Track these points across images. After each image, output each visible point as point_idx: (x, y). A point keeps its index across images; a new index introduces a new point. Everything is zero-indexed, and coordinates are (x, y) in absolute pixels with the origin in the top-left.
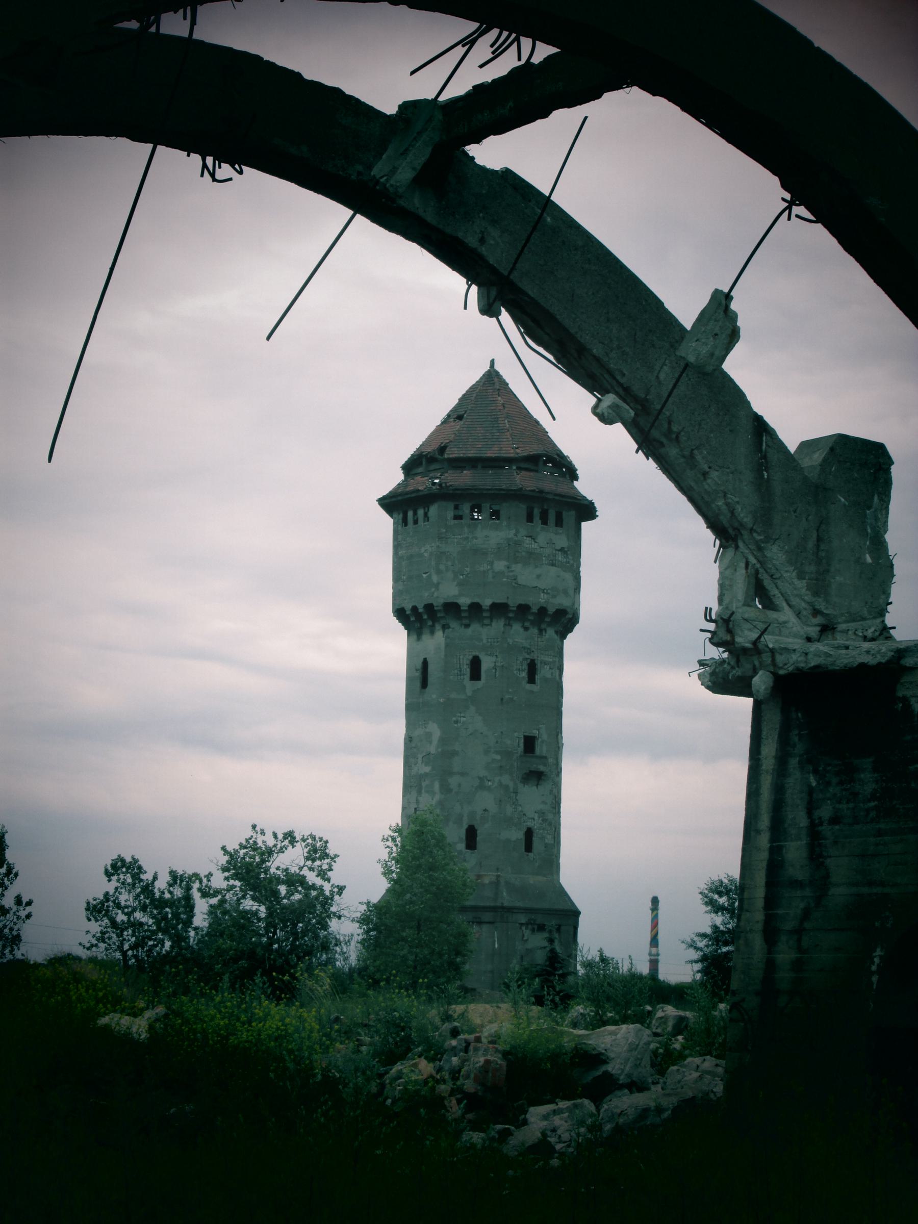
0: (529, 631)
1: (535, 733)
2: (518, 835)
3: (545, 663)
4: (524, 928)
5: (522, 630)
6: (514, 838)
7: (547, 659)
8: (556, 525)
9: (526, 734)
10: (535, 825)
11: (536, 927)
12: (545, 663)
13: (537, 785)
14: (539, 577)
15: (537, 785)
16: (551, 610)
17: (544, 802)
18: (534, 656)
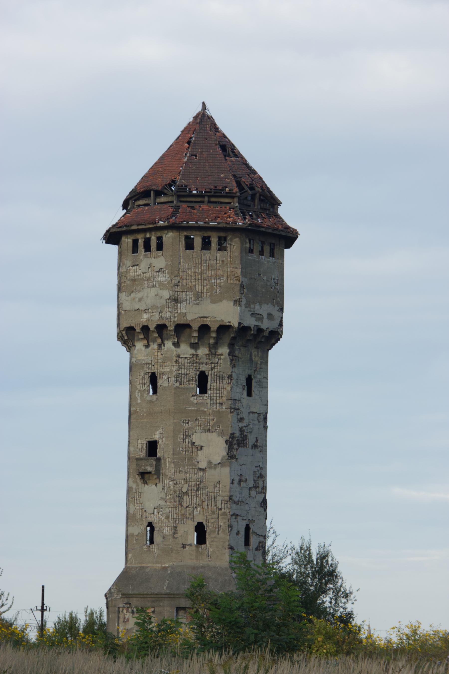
0: (150, 348)
1: (156, 437)
2: (139, 529)
3: (164, 374)
4: (125, 611)
5: (143, 348)
6: (136, 533)
7: (167, 369)
8: (145, 251)
9: (147, 440)
10: (154, 519)
11: (135, 610)
12: (164, 374)
13: (156, 485)
14: (140, 300)
15: (156, 485)
16: (152, 327)
17: (161, 498)
18: (154, 369)
